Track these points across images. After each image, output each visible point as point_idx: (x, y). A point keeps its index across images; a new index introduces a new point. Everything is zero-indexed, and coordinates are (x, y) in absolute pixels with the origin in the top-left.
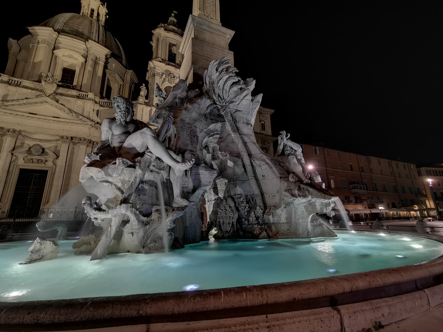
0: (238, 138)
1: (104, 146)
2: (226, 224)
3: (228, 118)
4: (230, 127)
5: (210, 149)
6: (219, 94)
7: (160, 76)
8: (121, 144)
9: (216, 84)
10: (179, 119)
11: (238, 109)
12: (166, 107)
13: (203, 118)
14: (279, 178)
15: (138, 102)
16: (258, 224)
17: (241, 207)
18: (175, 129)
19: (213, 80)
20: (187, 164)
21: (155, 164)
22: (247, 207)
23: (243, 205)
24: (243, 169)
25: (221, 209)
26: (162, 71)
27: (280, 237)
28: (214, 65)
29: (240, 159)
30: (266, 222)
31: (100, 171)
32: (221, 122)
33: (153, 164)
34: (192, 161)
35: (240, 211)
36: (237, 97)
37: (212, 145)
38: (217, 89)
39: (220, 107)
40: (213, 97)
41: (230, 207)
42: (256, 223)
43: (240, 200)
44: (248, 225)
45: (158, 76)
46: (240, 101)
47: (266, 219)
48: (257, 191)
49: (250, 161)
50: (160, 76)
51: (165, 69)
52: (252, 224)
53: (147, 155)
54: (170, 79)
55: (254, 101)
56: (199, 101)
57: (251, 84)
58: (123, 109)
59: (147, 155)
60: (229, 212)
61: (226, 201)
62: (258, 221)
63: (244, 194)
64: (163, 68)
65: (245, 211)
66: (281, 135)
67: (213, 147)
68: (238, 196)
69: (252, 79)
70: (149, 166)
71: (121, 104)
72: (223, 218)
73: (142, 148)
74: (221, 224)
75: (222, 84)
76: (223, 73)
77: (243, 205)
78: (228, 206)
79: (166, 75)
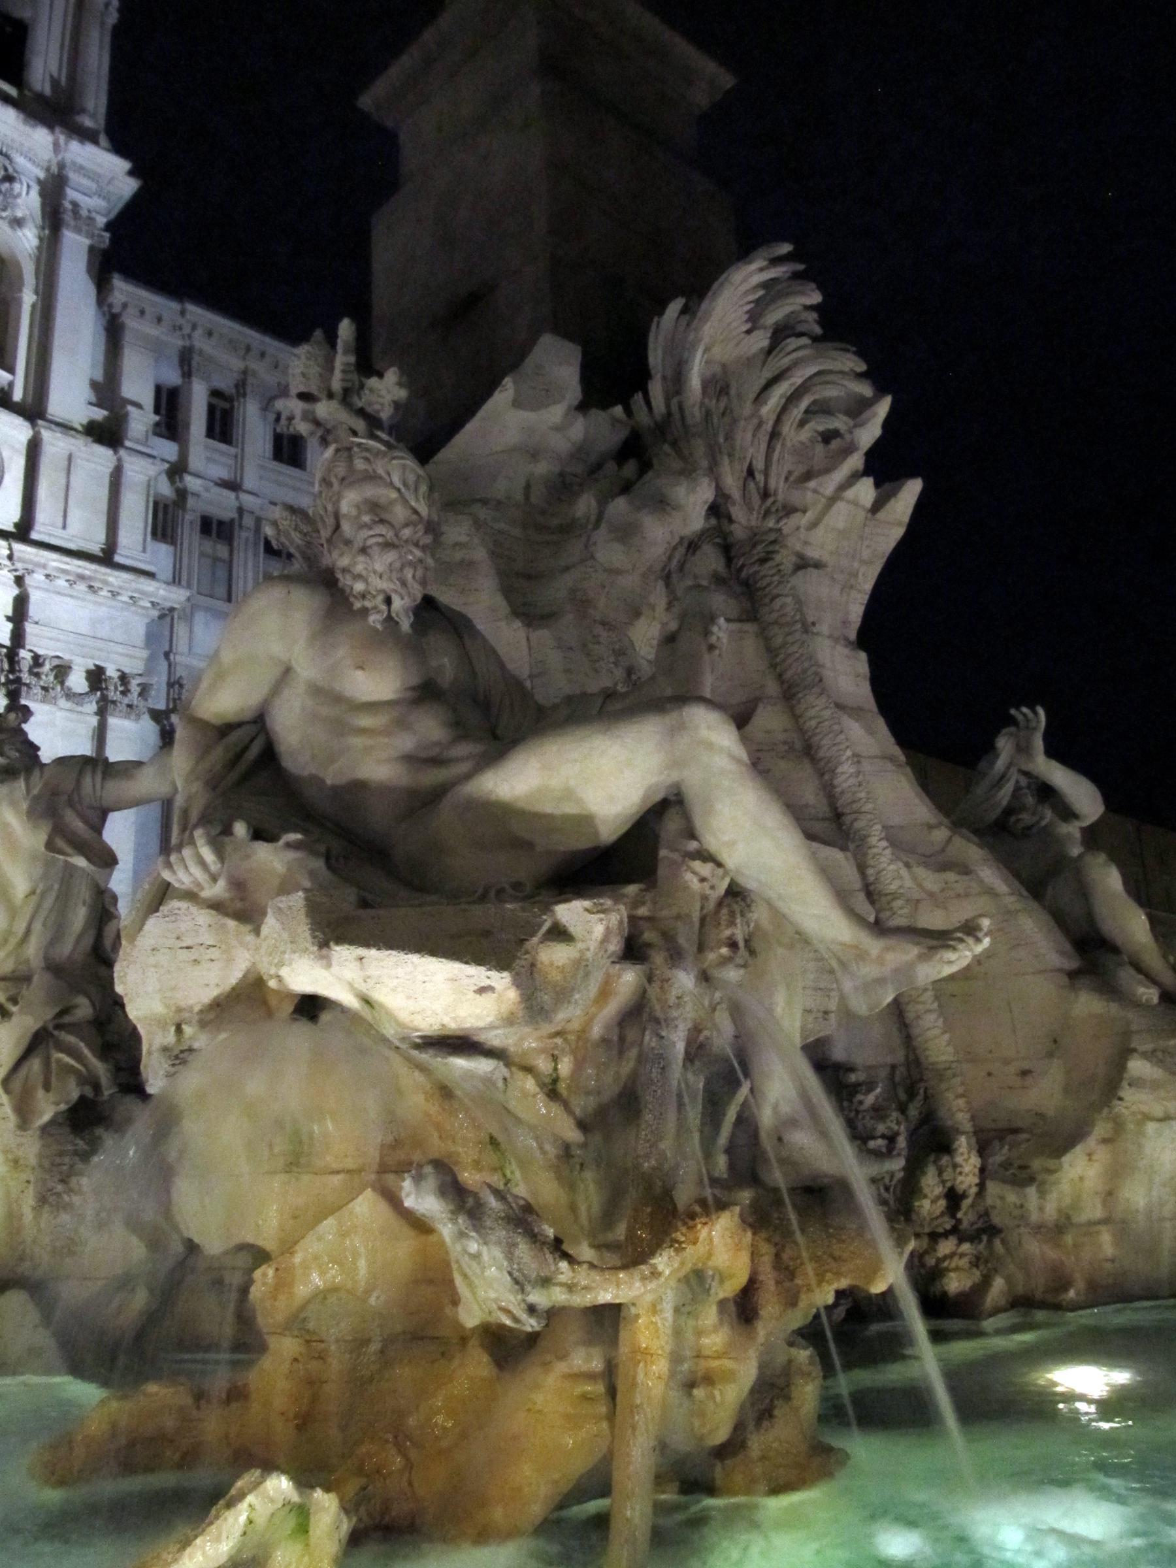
1: (242, 767)
23: (881, 1128)
36: (812, 484)
38: (751, 428)
39: (738, 532)
46: (820, 507)
53: (694, 873)
55: (881, 515)
58: (407, 533)
59: (694, 873)
66: (1012, 729)
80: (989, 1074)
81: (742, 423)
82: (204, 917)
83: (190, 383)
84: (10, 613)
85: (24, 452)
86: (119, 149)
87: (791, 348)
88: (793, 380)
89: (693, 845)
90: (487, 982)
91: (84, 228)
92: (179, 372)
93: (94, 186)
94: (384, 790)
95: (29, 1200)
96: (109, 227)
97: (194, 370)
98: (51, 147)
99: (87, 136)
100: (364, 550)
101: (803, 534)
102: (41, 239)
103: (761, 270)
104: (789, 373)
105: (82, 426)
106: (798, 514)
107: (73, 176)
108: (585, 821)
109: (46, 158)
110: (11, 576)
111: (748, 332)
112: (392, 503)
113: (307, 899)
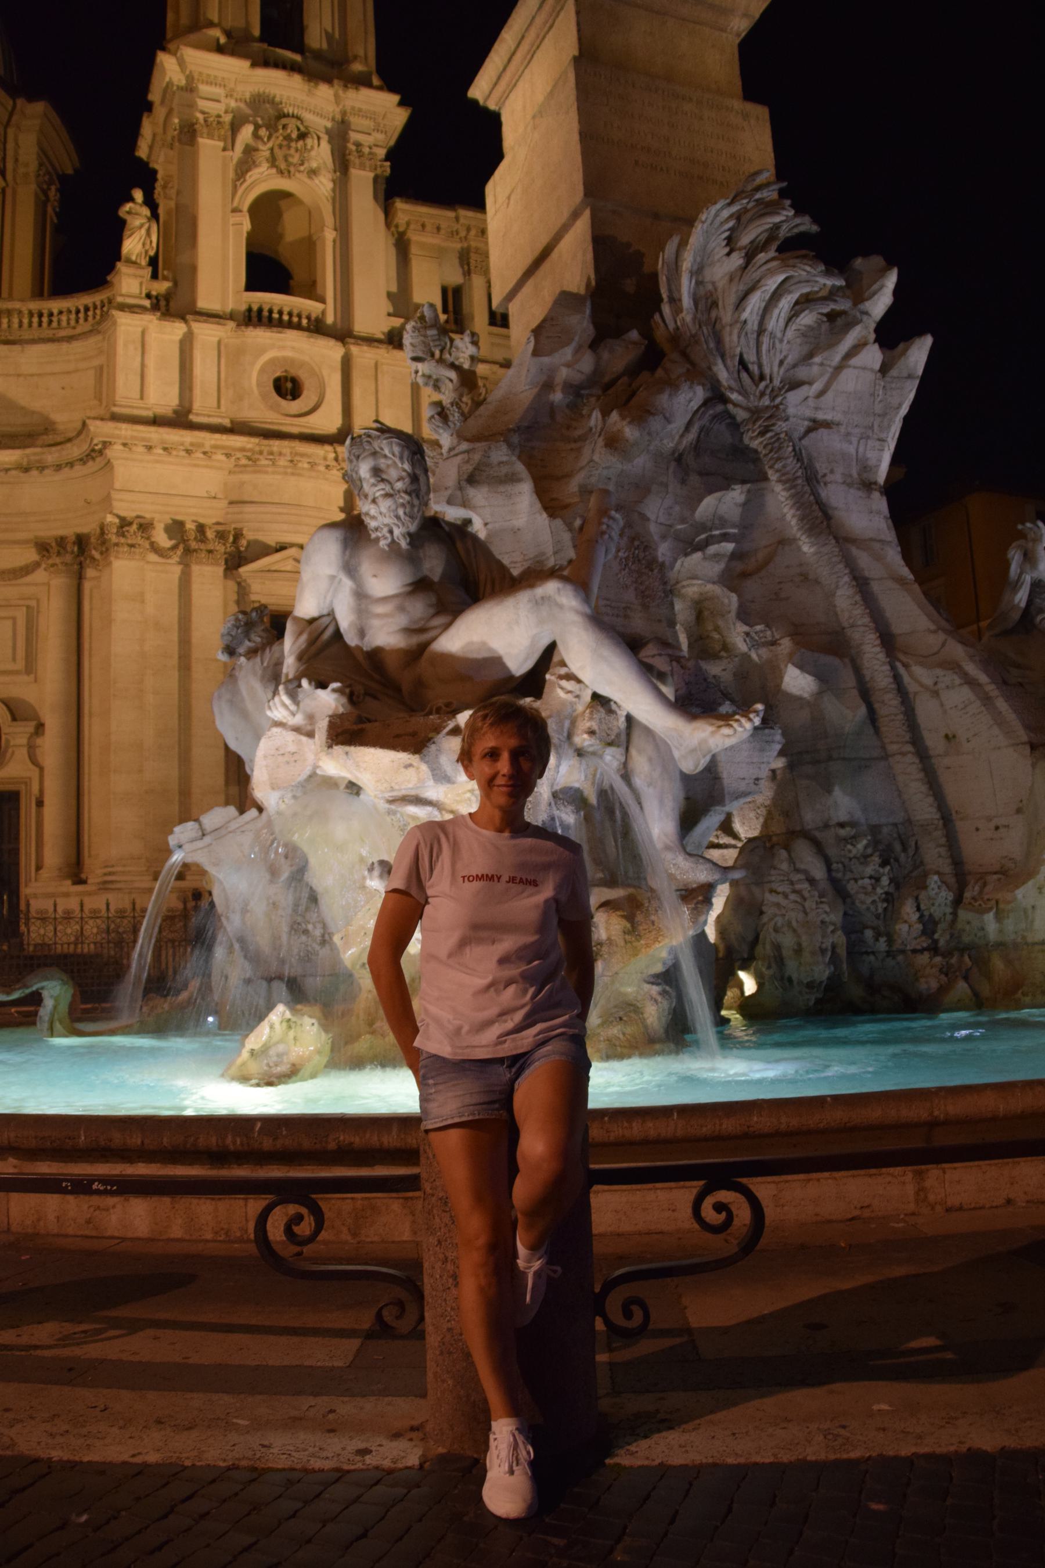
0: (834, 559)
1: (319, 643)
2: (813, 953)
3: (784, 467)
4: (792, 512)
5: (678, 606)
6: (741, 355)
7: (222, 132)
8: (415, 640)
9: (730, 309)
10: (573, 485)
11: (820, 416)
12: (510, 430)
13: (671, 470)
14: (1028, 748)
15: (110, 302)
16: (934, 949)
17: (856, 880)
18: (567, 537)
19: (710, 287)
20: (741, 726)
21: (594, 725)
22: (885, 881)
23: (869, 870)
24: (863, 710)
25: (778, 893)
26: (233, 104)
27: (1027, 1000)
28: (719, 219)
29: (847, 660)
30: (966, 939)
31: (411, 765)
32: (744, 482)
33: (585, 724)
34: (756, 712)
35: (849, 895)
36: (817, 359)
37: (695, 589)
38: (736, 332)
39: (741, 415)
40: (715, 369)
41: (811, 881)
42: (925, 945)
43: (854, 851)
44: (888, 956)
45: (211, 136)
47: (967, 927)
48: (924, 810)
49: (893, 668)
50: (222, 132)
51: (247, 91)
52: (903, 952)
53: (562, 688)
54: (280, 147)
55: (894, 372)
56: (663, 399)
57: (875, 287)
58: (399, 485)
59: (562, 688)
60: (817, 903)
61: (790, 855)
62: (931, 938)
63: (863, 821)
64: (240, 88)
65: (876, 898)
66: (1021, 542)
67: (696, 597)
68: (843, 832)
69: (878, 261)
70: (570, 736)
71: (390, 462)
72: (794, 931)
73: (526, 659)
74: (785, 953)
75: (756, 309)
76: (762, 257)
77: (869, 870)
78: (802, 876)
79: (257, 127)
80: (977, 829)
81: (728, 329)
82: (290, 736)
83: (470, 280)
84: (342, 504)
85: (339, 366)
86: (390, 86)
87: (758, 264)
88: (764, 288)
89: (563, 671)
90: (409, 762)
91: (368, 163)
92: (461, 270)
93: (372, 124)
94: (398, 651)
95: (285, 929)
96: (388, 157)
97: (472, 268)
98: (332, 98)
99: (362, 81)
100: (374, 501)
101: (811, 402)
102: (334, 181)
103: (729, 204)
104: (762, 282)
105: (384, 334)
106: (805, 388)
107: (355, 121)
108: (496, 662)
109: (331, 110)
110: (340, 474)
111: (728, 254)
112: (388, 466)
113: (330, 722)
